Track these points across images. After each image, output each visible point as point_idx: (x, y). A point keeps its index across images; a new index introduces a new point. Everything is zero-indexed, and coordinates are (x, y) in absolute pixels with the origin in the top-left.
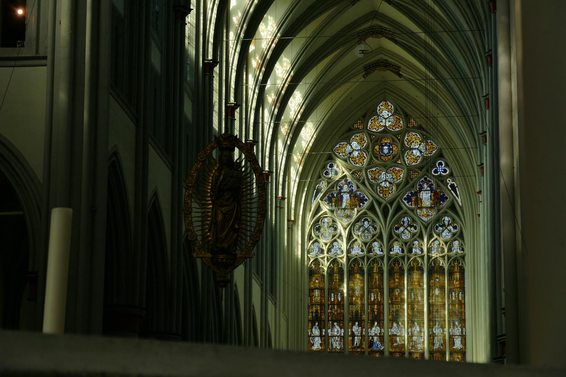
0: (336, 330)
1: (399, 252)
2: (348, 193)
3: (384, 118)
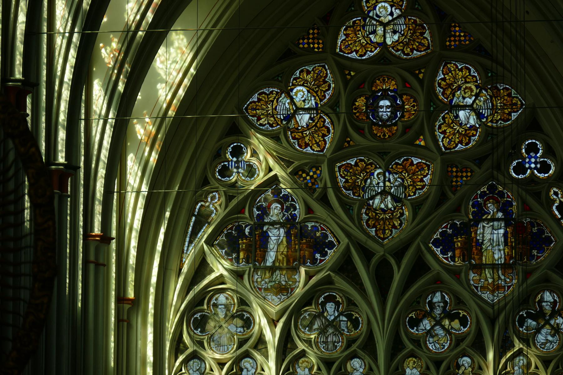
2: (282, 225)
3: (381, 23)
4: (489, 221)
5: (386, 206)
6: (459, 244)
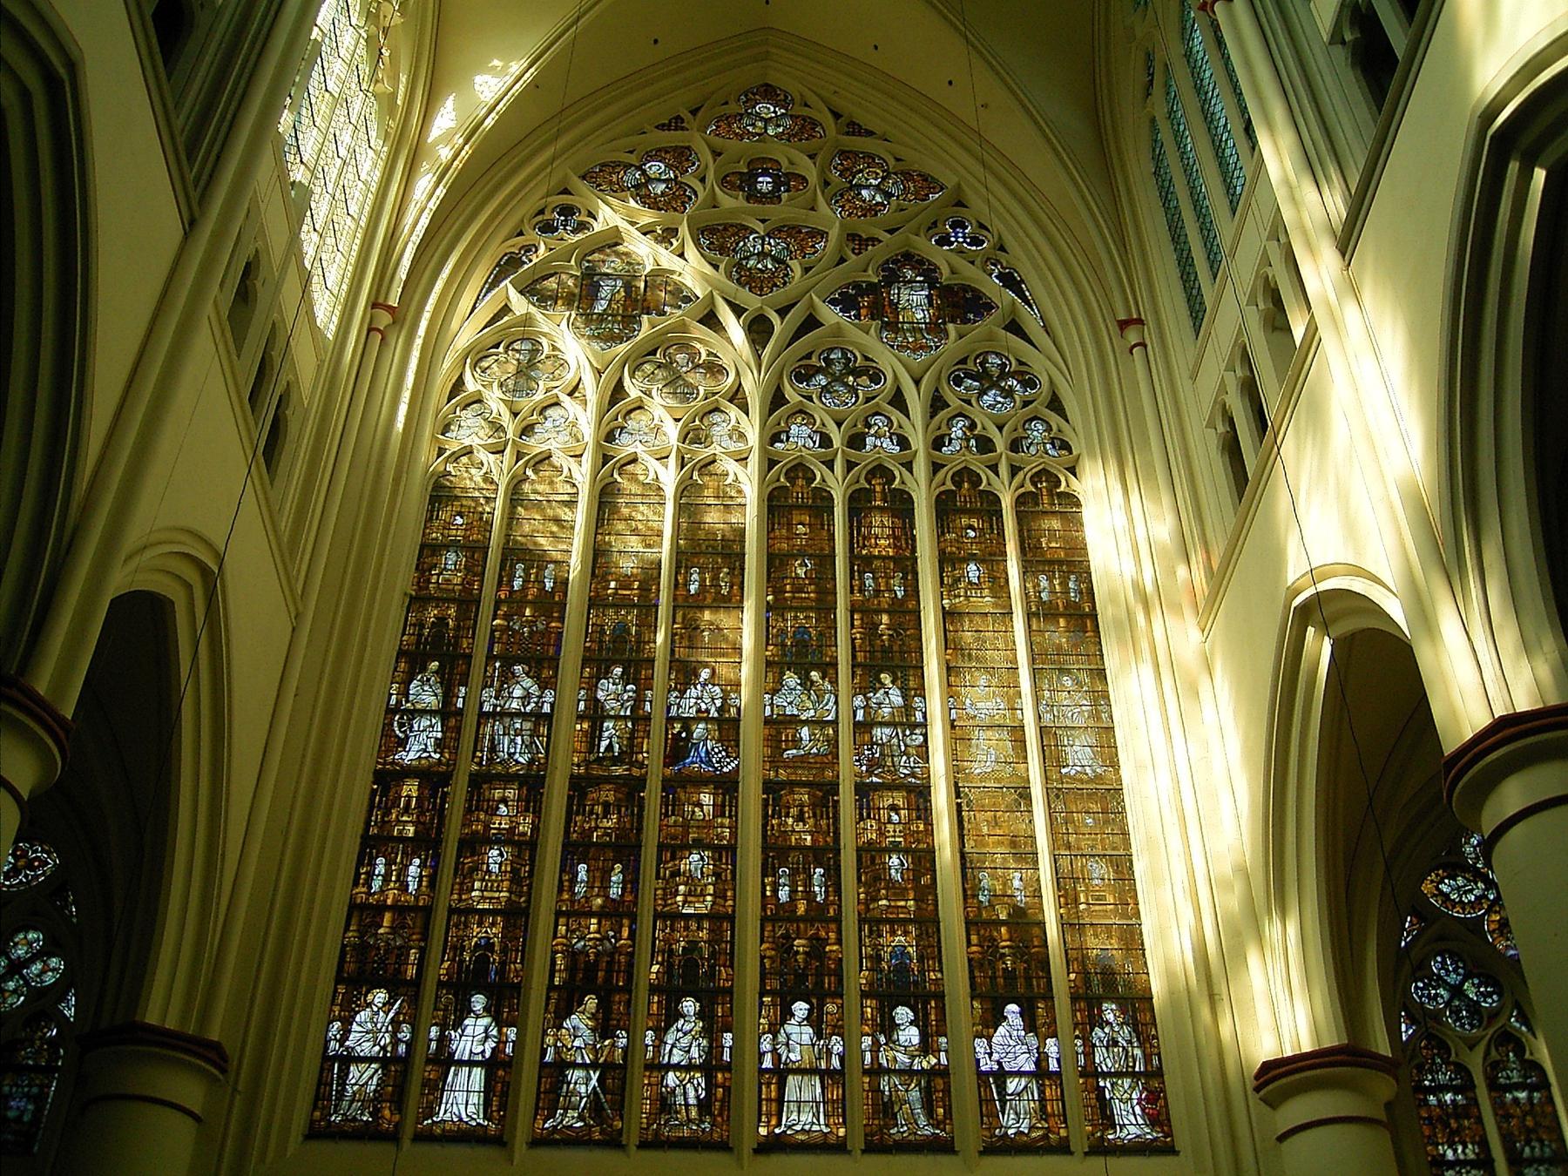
0: (518, 692)
4: (906, 283)
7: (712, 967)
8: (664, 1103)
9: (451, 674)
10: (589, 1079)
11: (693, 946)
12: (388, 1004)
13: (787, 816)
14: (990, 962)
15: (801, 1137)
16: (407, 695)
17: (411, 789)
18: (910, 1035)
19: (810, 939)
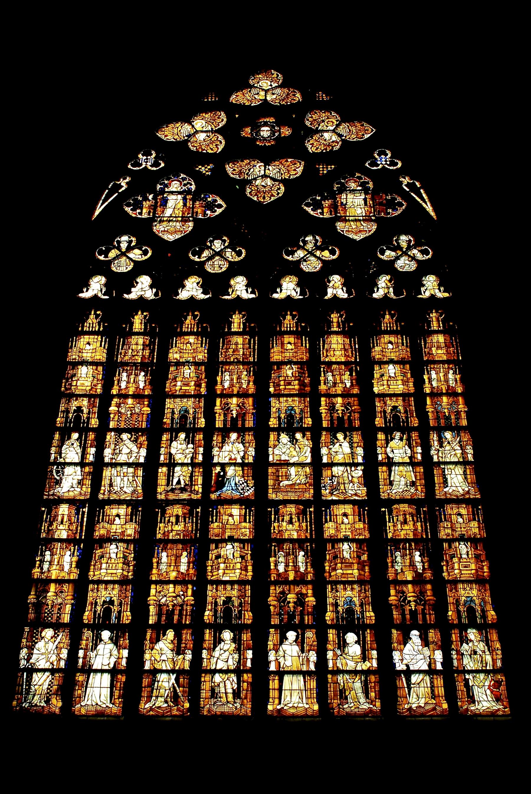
0: (125, 450)
1: (293, 294)
2: (179, 193)
5: (267, 184)
6: (327, 205)
7: (240, 612)
8: (214, 694)
9: (86, 440)
10: (169, 679)
11: (229, 599)
12: (55, 637)
13: (283, 520)
14: (402, 606)
15: (292, 711)
16: (60, 454)
17: (64, 509)
18: (355, 650)
19: (297, 594)
